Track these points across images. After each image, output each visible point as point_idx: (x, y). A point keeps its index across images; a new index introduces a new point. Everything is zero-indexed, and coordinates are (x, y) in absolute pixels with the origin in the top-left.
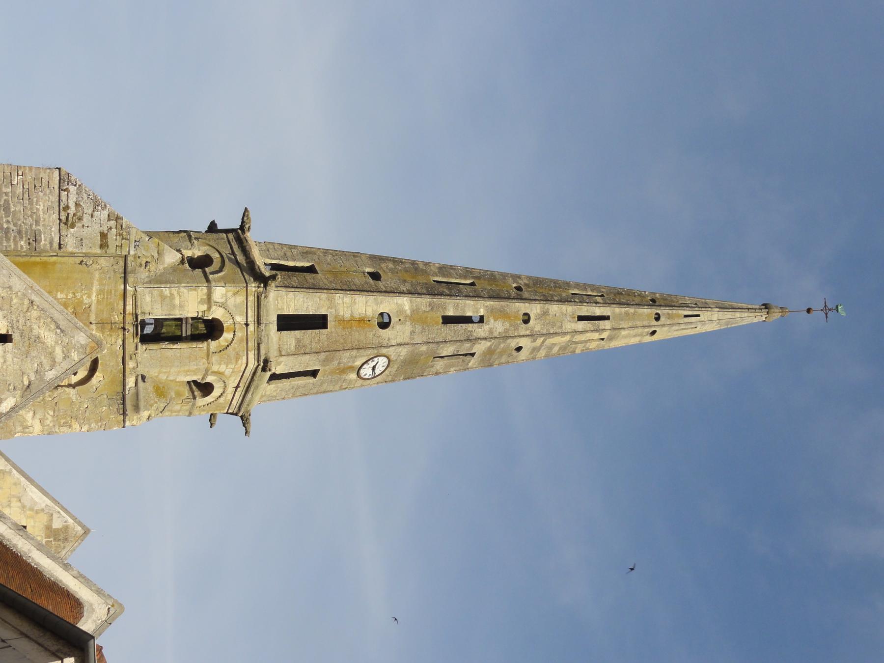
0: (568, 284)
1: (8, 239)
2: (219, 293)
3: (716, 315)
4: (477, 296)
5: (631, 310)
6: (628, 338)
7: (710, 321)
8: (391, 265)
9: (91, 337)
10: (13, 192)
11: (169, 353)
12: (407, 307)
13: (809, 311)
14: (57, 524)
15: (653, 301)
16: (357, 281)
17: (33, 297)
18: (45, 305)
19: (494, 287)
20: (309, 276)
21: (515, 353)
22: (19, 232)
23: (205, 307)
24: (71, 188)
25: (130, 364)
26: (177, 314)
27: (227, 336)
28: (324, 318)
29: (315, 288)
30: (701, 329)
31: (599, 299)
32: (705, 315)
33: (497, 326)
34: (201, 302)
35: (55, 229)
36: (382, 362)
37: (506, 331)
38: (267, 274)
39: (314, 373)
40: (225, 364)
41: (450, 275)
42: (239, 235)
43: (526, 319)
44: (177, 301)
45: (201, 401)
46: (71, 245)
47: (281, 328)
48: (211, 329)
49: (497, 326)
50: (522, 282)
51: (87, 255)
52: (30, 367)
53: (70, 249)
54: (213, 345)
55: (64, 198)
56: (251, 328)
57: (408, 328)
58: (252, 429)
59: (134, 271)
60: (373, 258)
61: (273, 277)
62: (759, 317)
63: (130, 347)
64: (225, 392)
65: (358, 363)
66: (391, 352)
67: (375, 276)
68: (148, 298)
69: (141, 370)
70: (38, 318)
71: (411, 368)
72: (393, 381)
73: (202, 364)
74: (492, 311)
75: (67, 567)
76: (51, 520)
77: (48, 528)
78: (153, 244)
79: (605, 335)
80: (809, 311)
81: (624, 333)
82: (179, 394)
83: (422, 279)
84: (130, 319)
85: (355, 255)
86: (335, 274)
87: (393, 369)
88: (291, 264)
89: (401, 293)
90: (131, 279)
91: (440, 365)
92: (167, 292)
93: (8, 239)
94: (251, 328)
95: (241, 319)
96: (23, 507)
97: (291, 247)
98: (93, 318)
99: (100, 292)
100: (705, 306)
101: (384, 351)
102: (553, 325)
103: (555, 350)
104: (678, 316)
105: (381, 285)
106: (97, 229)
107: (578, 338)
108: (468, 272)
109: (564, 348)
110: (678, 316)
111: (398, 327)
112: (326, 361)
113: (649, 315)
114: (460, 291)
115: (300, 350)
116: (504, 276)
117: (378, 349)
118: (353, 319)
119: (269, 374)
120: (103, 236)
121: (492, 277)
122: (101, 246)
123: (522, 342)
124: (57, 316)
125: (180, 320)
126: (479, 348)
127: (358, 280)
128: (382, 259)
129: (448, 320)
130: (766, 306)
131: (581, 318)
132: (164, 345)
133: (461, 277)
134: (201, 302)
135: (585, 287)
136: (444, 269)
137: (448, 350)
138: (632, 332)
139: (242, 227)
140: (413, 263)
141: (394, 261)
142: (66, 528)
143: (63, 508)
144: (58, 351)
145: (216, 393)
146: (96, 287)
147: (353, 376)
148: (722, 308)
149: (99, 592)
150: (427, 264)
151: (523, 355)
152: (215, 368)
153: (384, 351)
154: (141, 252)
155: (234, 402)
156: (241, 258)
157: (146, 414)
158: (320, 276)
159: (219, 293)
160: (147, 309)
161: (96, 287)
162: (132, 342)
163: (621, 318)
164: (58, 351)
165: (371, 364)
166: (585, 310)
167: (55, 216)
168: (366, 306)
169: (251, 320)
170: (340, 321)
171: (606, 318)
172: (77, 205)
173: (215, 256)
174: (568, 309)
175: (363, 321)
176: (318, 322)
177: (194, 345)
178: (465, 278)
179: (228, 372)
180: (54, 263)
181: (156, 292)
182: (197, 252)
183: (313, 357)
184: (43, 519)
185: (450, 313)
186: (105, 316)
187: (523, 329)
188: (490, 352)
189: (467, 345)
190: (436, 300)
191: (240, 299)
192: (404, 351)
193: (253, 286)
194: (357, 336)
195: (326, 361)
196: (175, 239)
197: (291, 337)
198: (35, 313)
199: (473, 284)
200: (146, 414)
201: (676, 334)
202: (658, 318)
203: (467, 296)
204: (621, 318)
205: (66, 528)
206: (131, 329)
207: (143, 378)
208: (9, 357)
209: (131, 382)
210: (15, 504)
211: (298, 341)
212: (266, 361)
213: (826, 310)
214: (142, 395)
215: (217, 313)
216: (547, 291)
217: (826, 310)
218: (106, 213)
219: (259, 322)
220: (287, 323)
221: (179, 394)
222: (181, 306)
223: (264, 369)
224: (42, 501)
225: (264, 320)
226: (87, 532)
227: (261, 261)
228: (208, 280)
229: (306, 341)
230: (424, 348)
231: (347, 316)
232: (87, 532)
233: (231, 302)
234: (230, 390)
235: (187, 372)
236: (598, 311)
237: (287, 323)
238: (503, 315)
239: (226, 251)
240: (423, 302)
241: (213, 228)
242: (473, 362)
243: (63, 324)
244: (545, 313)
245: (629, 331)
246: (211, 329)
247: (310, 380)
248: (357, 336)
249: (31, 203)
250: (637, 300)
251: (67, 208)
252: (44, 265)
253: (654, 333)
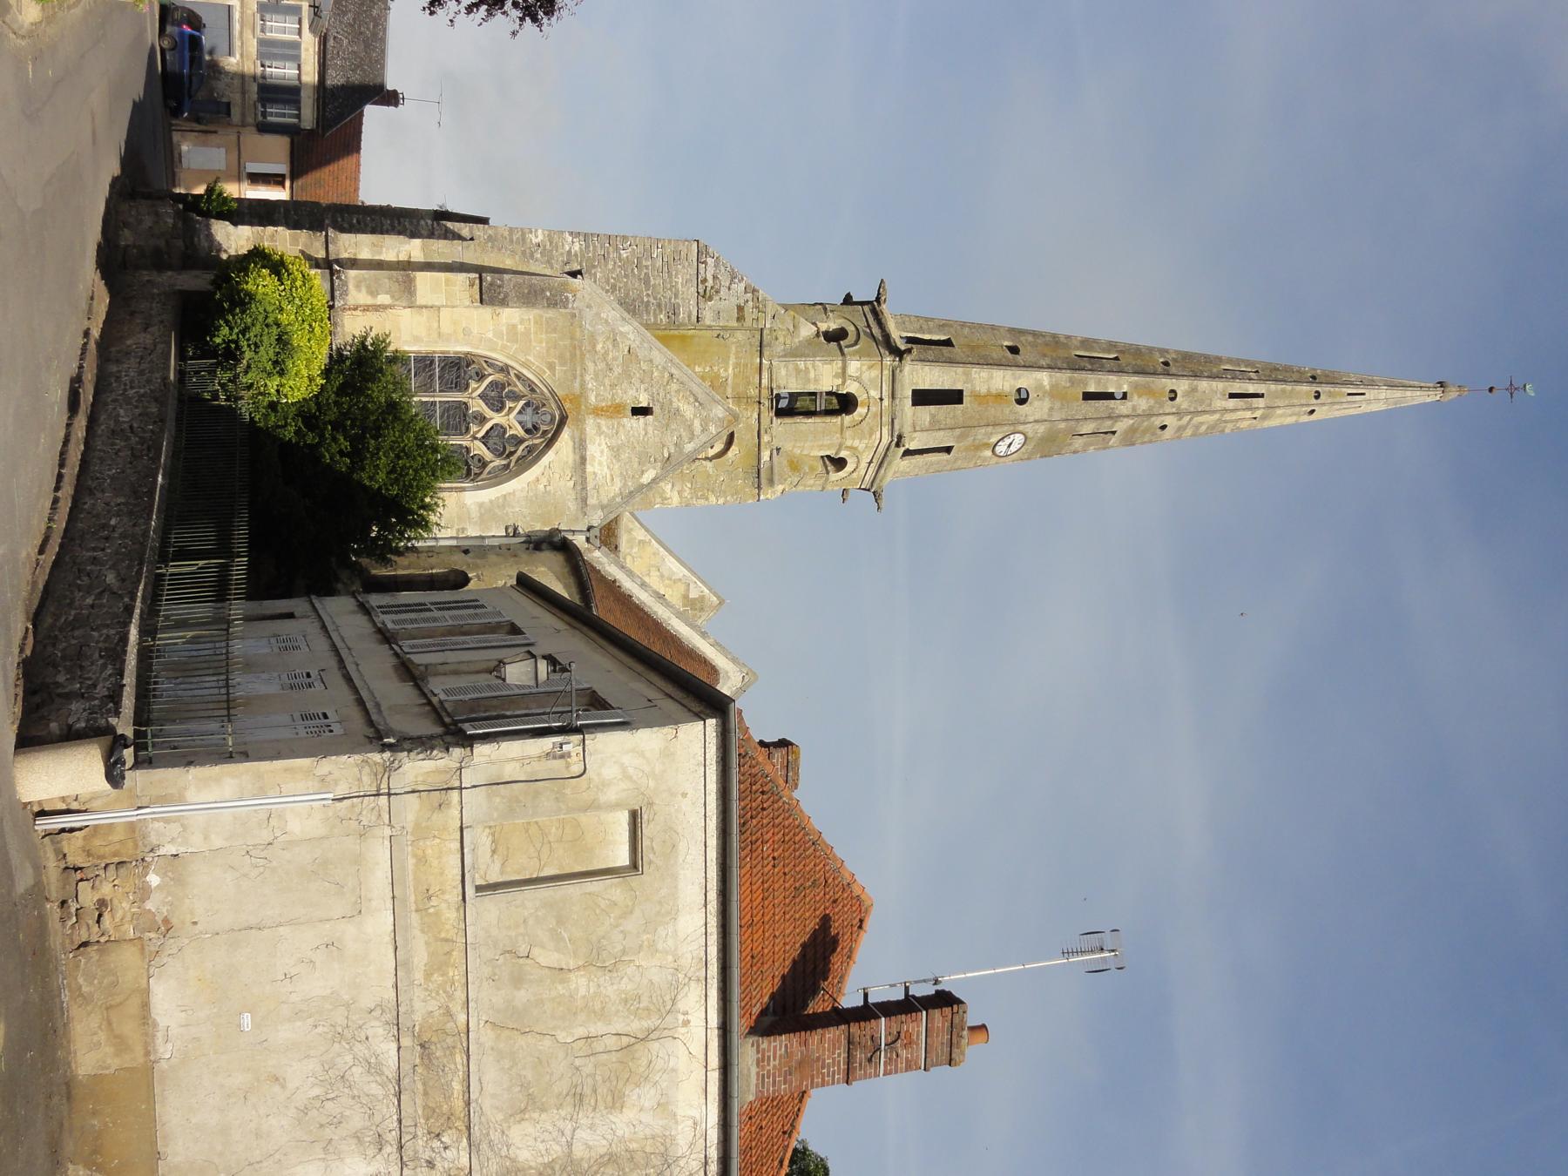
0: (1219, 360)
1: (648, 313)
2: (854, 366)
3: (1384, 393)
4: (1121, 371)
5: (1289, 388)
6: (1284, 418)
7: (1377, 400)
8: (1030, 338)
9: (728, 410)
10: (653, 265)
11: (803, 427)
12: (1046, 383)
13: (1491, 390)
14: (692, 595)
15: (1314, 377)
16: (994, 355)
17: (673, 371)
18: (685, 379)
19: (1139, 362)
20: (945, 349)
21: (1159, 432)
22: (659, 305)
23: (840, 381)
24: (709, 260)
25: (765, 438)
26: (811, 389)
27: (861, 410)
28: (961, 392)
29: (951, 362)
30: (1365, 408)
31: (1253, 375)
32: (1371, 393)
33: (1141, 403)
34: (836, 376)
35: (693, 302)
36: (1019, 438)
37: (1151, 408)
38: (903, 347)
39: (948, 450)
40: (858, 439)
41: (1091, 349)
42: (874, 308)
43: (1173, 395)
44: (812, 375)
45: (835, 476)
46: (708, 318)
47: (915, 403)
48: (846, 404)
49: (1141, 403)
50: (1169, 357)
51: (724, 328)
52: (670, 440)
53: (708, 323)
54: (847, 419)
55: (702, 271)
56: (886, 403)
57: (1047, 404)
58: (883, 505)
59: (769, 345)
60: (1012, 331)
61: (909, 351)
62: (1434, 396)
64: (858, 469)
65: (994, 440)
66: (1028, 428)
67: (1014, 350)
68: (783, 372)
69: (776, 444)
70: (678, 391)
71: (1048, 445)
73: (836, 438)
74: (1136, 387)
75: (704, 635)
76: (688, 590)
77: (686, 597)
78: (788, 318)
79: (1258, 414)
80: (1491, 390)
81: (1279, 412)
82: (812, 469)
83: (1062, 353)
84: (765, 393)
85: (993, 327)
86: (973, 348)
87: (1029, 447)
88: (927, 337)
89: (1041, 367)
90: (766, 353)
91: (1078, 443)
92: (802, 365)
93: (648, 313)
94: (886, 403)
95: (875, 394)
96: (662, 576)
97: (927, 320)
98: (729, 392)
99: (737, 365)
100: (1372, 384)
101: (1021, 428)
102: (1201, 402)
103: (1203, 428)
104: (1341, 394)
105: (1019, 359)
106: (734, 301)
107: (1228, 417)
108: (1111, 346)
109: (1212, 427)
110: (1341, 394)
111: (1036, 403)
112: (960, 438)
113: (1307, 393)
114: (1102, 366)
115: (935, 426)
116: (1151, 350)
117: (1015, 425)
118: (989, 394)
119: (902, 450)
120: (740, 309)
121: (1137, 351)
122: (738, 319)
123: (1168, 420)
124: (695, 389)
125: (814, 394)
126: (1120, 426)
127: (997, 354)
128: (1022, 332)
129: (1088, 396)
130: (1442, 384)
131: (1232, 396)
132: (799, 419)
133: (1104, 351)
134: (836, 376)
135: (1238, 362)
136: (1086, 343)
137: (1088, 428)
138: (1289, 411)
139: (878, 299)
140: (1054, 336)
141: (1034, 334)
142: (702, 598)
143: (699, 578)
144: (697, 423)
146: (732, 361)
147: (988, 453)
148: (1392, 386)
149: (734, 660)
150: (1068, 337)
151: (1168, 433)
152: (849, 443)
153: (1021, 428)
154: (778, 324)
156: (876, 331)
157: (780, 488)
158: (957, 349)
159: (854, 366)
160: (782, 383)
161: (732, 361)
162: (768, 415)
163: (1276, 395)
164: (697, 423)
165: (1007, 441)
166: (1238, 387)
167: (693, 289)
168: (1003, 380)
169: (886, 394)
170: (977, 396)
171: (1262, 396)
172: (715, 277)
173: (851, 329)
174: (1219, 385)
175: (1000, 396)
176: (954, 397)
177: (828, 419)
178: (1109, 352)
179: (861, 446)
180: (693, 337)
181: (791, 366)
182: (832, 325)
183: (948, 433)
184: (682, 588)
185: (1092, 390)
186: (741, 389)
187: (1169, 407)
188: (1132, 430)
189: (1109, 423)
190: (1077, 375)
191: (875, 373)
192: (1041, 429)
193: (889, 360)
194: (993, 412)
195: (960, 438)
196: (811, 312)
197: (926, 412)
198: (674, 386)
199: (1116, 359)
200: (780, 488)
201: (1338, 414)
202: (1317, 396)
203: (1111, 371)
204: (1276, 395)
205: (702, 598)
206: (767, 403)
207: (778, 450)
208: (650, 429)
209: (765, 456)
210: (655, 573)
211: (933, 416)
212: (900, 437)
213: (1512, 389)
214: (776, 470)
215: (851, 388)
216: (1197, 366)
217: (1512, 389)
218: (742, 285)
219: (893, 397)
220: (922, 398)
221: (812, 469)
222: (816, 380)
223: (898, 445)
225: (898, 395)
227: (896, 335)
228: (843, 354)
229: (941, 417)
230: (1062, 425)
231: (984, 391)
233: (866, 376)
234: (864, 465)
235: (821, 447)
236: (1251, 389)
237: (922, 398)
238: (1148, 391)
239: (861, 324)
240: (1063, 377)
241: (848, 300)
242: (1114, 440)
243: (701, 397)
244: (1194, 390)
245: (1285, 410)
246: (846, 404)
247: (944, 456)
248: (993, 412)
249: (670, 276)
250: (1296, 376)
251: (705, 280)
252: (683, 338)
253: (1312, 412)
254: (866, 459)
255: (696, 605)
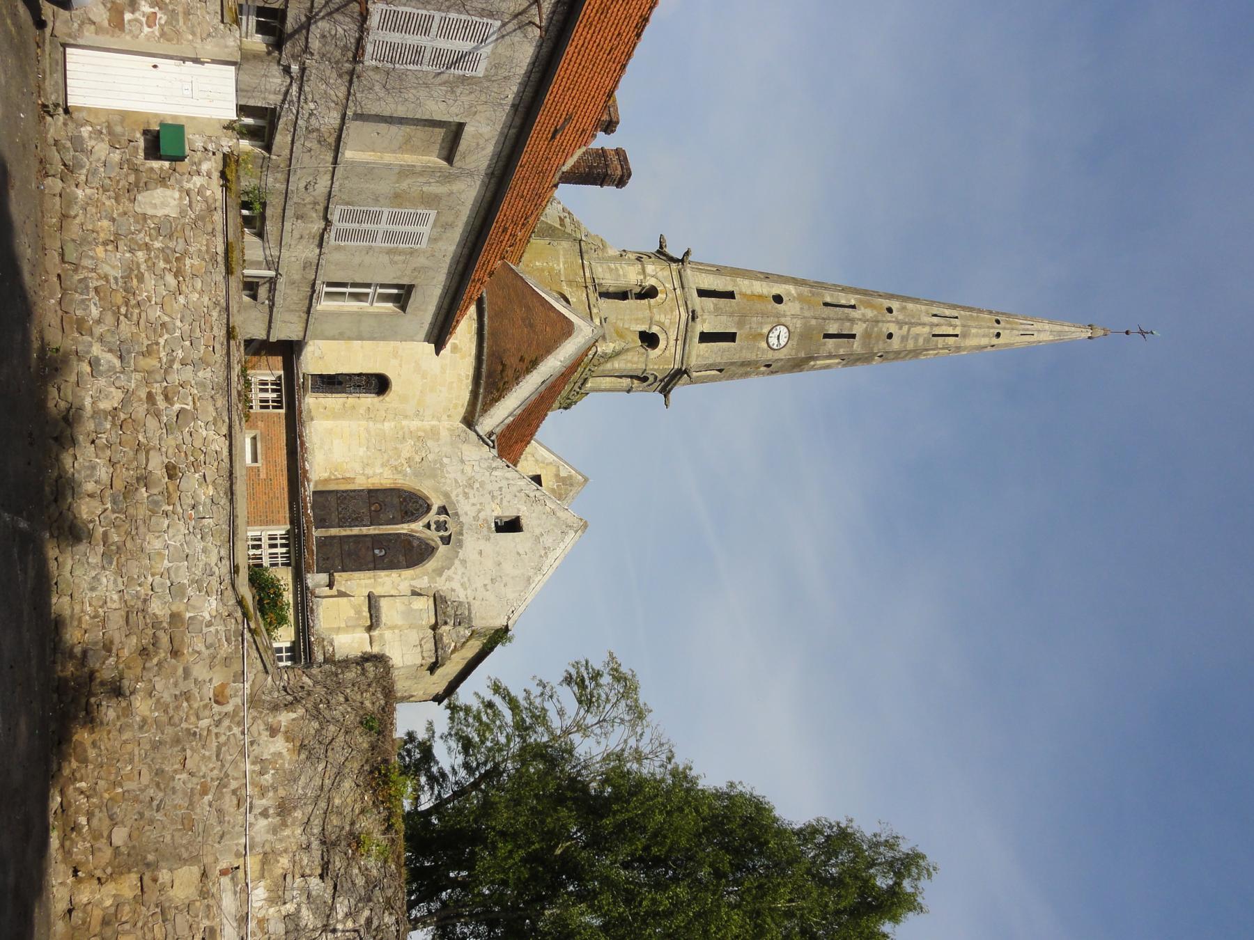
7: (1045, 332)
13: (1127, 333)
14: (563, 474)
25: (595, 311)
27: (661, 296)
33: (870, 313)
34: (639, 273)
48: (651, 293)
49: (870, 313)
54: (652, 301)
56: (678, 291)
63: (593, 301)
65: (765, 331)
72: (797, 365)
77: (557, 475)
90: (586, 257)
94: (678, 291)
96: (537, 461)
101: (783, 320)
134: (639, 273)
139: (661, 247)
142: (570, 477)
145: (662, 344)
147: (764, 345)
155: (677, 357)
165: (776, 333)
166: (935, 310)
170: (744, 295)
175: (760, 296)
185: (828, 300)
191: (667, 273)
195: (741, 324)
215: (651, 282)
219: (683, 287)
224: (551, 458)
225: (686, 285)
226: (586, 480)
231: (749, 292)
232: (586, 480)
233: (660, 274)
234: (672, 342)
235: (637, 320)
246: (651, 293)
248: (759, 306)
254: (673, 337)
255: (566, 482)
